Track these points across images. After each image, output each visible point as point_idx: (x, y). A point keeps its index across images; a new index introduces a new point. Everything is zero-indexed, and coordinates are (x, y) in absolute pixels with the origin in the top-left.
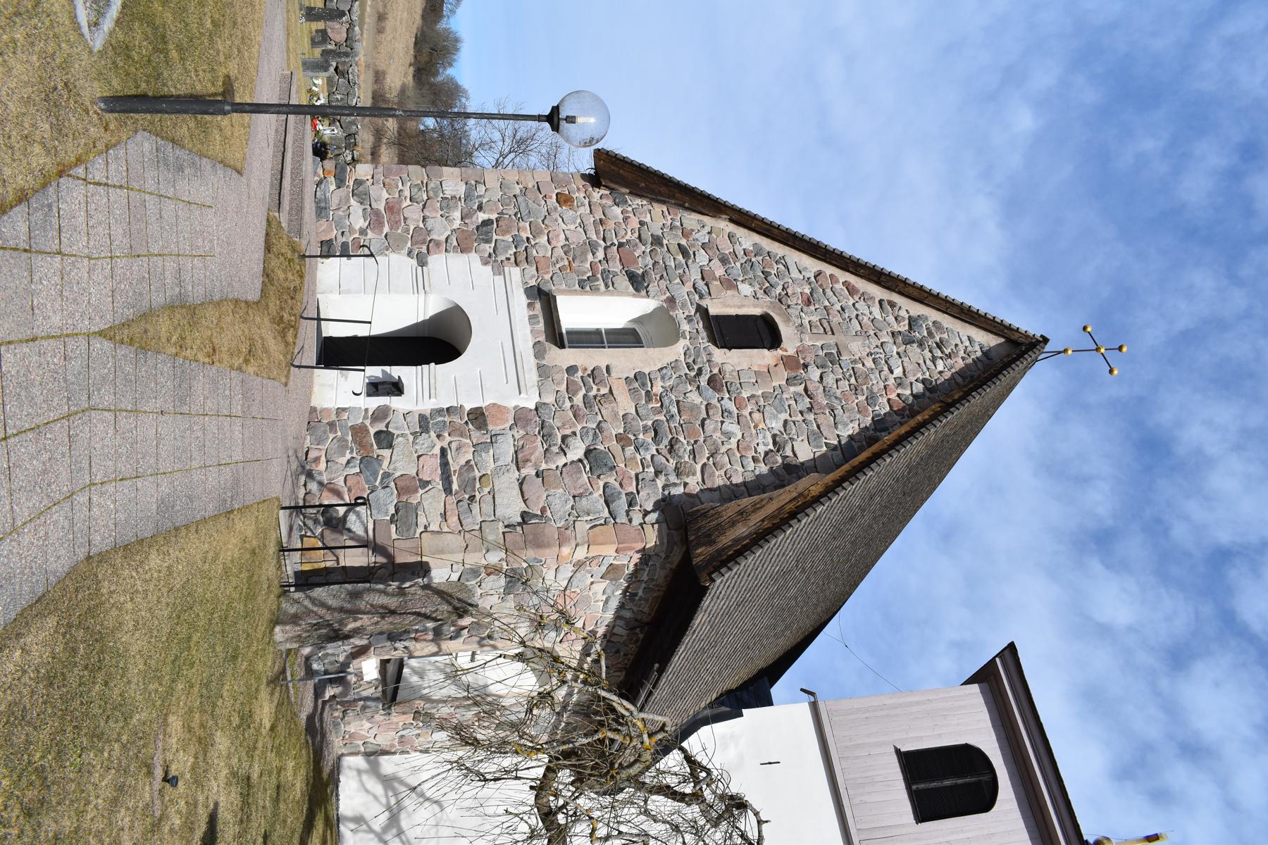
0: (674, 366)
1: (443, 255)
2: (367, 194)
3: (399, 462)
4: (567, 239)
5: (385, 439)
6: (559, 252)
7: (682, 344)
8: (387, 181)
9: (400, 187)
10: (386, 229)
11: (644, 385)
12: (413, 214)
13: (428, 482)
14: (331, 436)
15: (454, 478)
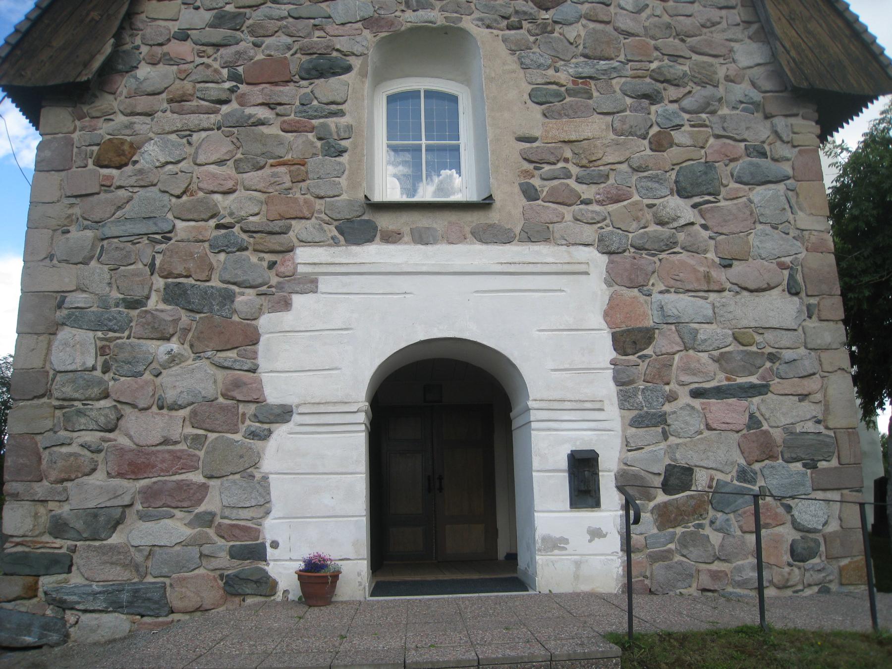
1: (265, 377)
2: (94, 514)
3: (716, 460)
4: (221, 163)
5: (677, 478)
6: (253, 178)
8: (54, 475)
9: (74, 449)
10: (196, 477)
12: (143, 429)
13: (752, 416)
14: (678, 558)
15: (740, 380)
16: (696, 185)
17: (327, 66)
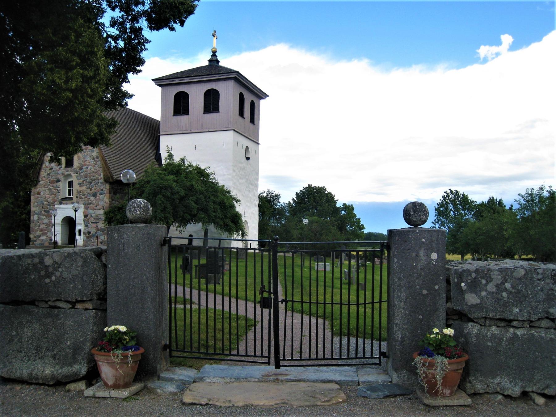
0: (77, 177)
3: (93, 231)
6: (51, 196)
12: (42, 226)
16: (94, 195)
17: (58, 181)
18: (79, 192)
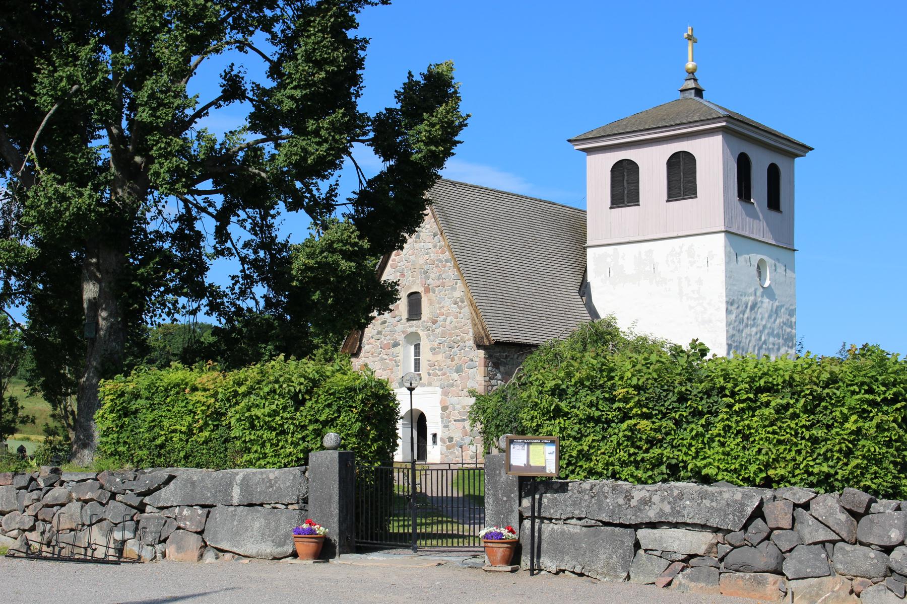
0: (428, 336)
3: (457, 436)
7: (421, 333)
11: (435, 349)
16: (459, 370)
17: (396, 345)
18: (432, 365)
